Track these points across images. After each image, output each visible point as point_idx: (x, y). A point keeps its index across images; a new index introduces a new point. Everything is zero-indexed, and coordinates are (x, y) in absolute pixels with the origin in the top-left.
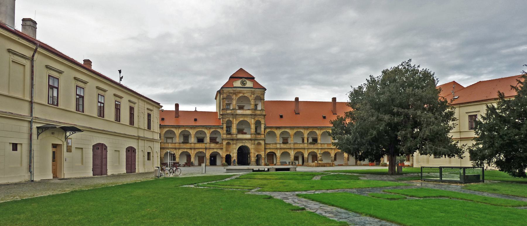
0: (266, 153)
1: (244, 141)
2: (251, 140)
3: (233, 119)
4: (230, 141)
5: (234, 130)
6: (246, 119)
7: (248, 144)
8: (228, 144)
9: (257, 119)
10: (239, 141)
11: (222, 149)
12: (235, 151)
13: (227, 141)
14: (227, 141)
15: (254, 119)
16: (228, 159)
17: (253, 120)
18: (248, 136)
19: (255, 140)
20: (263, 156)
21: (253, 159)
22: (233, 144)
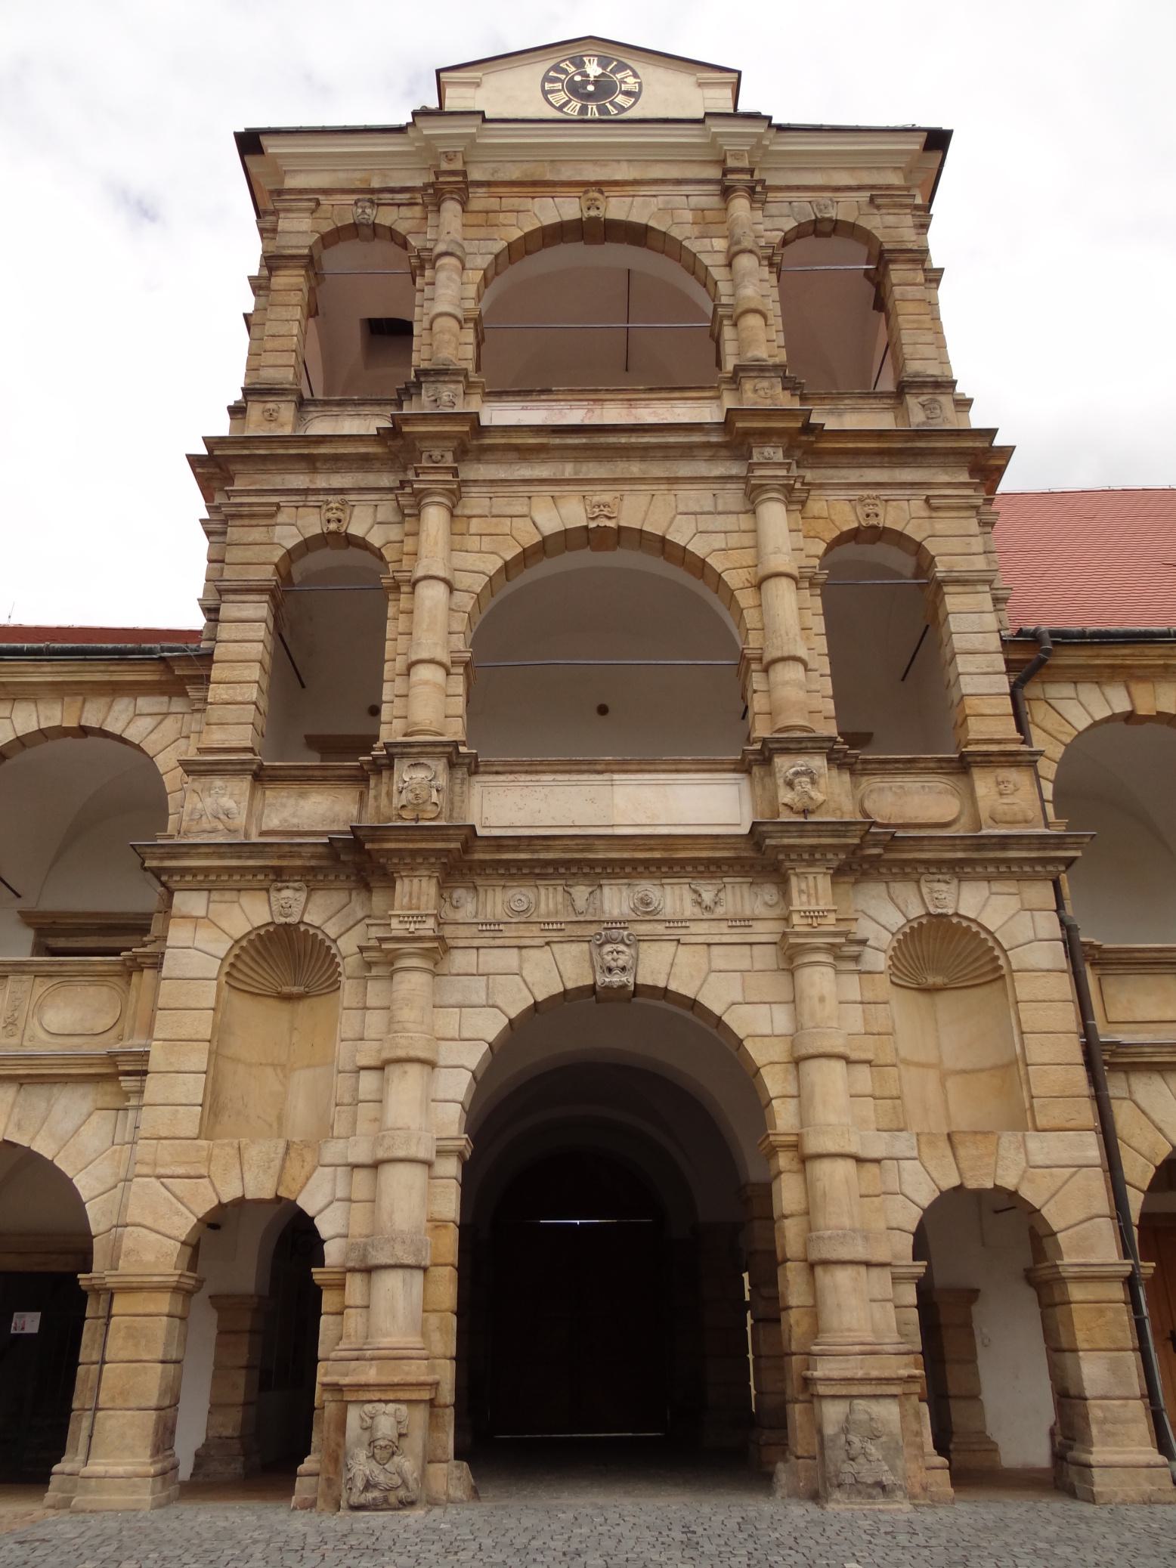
0: (1139, 1172)
1: (616, 900)
2: (759, 857)
3: (410, 513)
4: (321, 912)
5: (424, 699)
6: (639, 509)
7: (704, 958)
8: (286, 965)
9: (839, 511)
10: (498, 901)
11: (119, 1074)
12: (431, 1111)
13: (249, 913)
14: (249, 913)
15: (794, 497)
16: (270, 1283)
17: (774, 514)
18: (705, 803)
19: (868, 855)
20: (1088, 1237)
21: (855, 1317)
22: (382, 960)
